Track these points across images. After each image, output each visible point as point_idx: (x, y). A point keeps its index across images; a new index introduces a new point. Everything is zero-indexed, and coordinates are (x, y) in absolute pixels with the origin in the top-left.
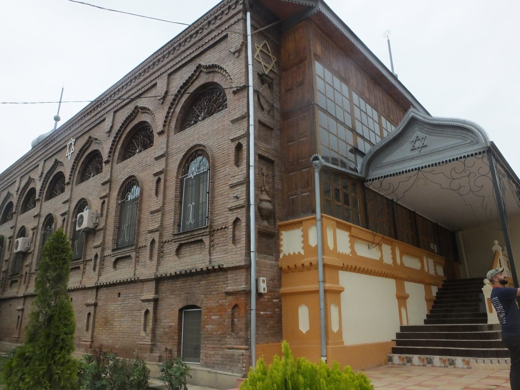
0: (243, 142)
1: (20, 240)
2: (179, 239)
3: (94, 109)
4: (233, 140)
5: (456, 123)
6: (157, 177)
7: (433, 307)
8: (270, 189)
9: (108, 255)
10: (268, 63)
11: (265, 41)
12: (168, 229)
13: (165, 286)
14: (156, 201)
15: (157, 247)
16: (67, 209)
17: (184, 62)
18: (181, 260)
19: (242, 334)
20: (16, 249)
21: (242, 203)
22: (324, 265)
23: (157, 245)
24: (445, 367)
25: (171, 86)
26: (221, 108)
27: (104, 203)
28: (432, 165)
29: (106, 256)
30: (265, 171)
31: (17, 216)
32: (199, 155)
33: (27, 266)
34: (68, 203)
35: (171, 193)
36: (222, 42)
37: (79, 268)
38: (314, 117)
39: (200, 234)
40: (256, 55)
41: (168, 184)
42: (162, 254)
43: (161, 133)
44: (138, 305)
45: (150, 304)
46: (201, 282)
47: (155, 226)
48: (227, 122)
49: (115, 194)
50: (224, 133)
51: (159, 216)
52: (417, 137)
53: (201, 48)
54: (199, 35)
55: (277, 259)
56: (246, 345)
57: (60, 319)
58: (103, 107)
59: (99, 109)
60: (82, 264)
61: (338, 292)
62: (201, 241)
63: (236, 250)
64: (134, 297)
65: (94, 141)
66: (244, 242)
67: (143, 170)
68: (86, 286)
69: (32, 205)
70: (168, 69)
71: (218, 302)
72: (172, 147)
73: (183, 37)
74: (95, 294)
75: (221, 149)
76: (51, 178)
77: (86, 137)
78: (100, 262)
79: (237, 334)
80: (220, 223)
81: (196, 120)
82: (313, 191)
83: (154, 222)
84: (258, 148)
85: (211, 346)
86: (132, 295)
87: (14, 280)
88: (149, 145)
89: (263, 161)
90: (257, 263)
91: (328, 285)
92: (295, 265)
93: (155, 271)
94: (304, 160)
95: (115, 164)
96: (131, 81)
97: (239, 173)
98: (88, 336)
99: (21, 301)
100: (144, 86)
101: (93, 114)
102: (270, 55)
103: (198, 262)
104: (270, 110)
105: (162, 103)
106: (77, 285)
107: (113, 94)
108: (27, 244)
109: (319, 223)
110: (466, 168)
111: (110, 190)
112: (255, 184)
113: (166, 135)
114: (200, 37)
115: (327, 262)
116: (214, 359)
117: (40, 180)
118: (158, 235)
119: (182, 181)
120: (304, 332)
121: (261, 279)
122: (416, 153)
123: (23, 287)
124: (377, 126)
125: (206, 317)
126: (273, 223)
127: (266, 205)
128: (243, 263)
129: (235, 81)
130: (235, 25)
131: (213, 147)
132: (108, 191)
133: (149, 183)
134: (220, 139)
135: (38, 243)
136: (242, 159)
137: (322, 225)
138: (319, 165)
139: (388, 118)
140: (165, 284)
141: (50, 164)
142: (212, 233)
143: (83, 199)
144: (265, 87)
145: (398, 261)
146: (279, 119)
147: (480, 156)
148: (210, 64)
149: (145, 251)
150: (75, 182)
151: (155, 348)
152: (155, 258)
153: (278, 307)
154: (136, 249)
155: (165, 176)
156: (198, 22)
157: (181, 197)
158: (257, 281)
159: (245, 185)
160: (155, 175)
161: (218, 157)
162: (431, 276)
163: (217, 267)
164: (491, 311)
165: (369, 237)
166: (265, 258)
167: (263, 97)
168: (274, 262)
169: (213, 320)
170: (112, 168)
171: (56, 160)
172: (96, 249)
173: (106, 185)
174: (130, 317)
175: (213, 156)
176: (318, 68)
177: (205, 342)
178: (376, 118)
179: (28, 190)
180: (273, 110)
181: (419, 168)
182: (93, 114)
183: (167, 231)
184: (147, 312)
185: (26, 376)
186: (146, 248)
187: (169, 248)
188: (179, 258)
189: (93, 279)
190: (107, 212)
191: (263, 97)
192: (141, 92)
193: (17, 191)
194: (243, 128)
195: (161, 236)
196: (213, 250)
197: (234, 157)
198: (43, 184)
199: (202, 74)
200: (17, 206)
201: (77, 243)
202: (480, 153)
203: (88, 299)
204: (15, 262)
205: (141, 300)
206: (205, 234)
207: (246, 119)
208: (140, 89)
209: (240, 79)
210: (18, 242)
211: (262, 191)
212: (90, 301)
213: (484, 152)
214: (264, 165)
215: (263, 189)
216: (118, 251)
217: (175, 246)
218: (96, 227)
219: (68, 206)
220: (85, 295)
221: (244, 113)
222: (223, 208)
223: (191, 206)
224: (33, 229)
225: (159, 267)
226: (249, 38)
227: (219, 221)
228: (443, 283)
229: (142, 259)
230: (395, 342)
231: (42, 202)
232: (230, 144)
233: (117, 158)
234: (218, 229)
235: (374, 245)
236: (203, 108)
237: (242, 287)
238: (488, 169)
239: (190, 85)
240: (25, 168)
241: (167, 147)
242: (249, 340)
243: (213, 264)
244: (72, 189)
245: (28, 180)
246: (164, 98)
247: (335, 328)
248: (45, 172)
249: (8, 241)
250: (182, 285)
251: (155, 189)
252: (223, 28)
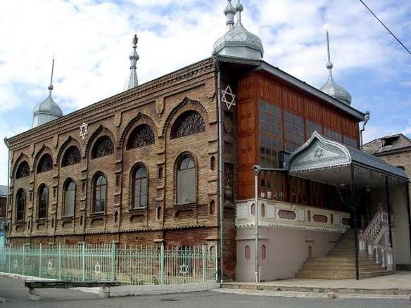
0: (216, 156)
13: (169, 235)
37: (102, 219)
111: (122, 168)
127: (229, 192)
128: (216, 225)
141: (64, 139)
193: (33, 154)
249: (28, 193)
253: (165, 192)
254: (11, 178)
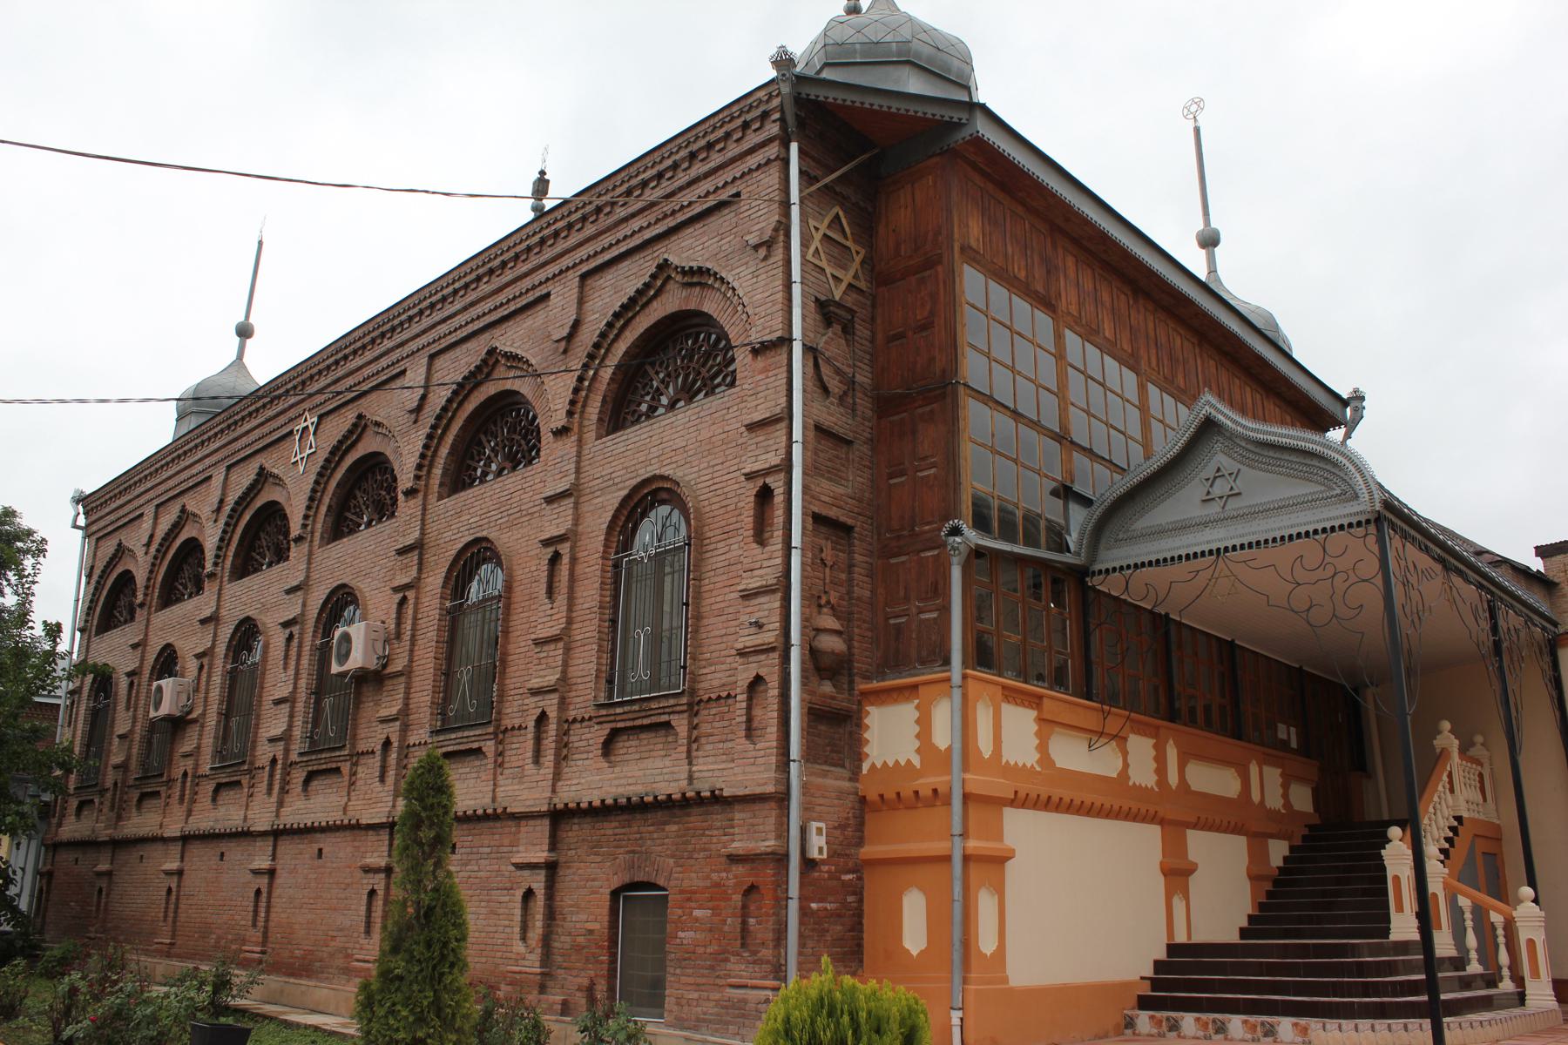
0: (776, 483)
1: (167, 684)
2: (612, 718)
3: (373, 341)
4: (750, 476)
5: (1307, 445)
6: (551, 549)
7: (1270, 894)
8: (841, 598)
9: (420, 743)
10: (844, 268)
11: (837, 209)
12: (580, 687)
13: (574, 832)
14: (549, 612)
15: (554, 733)
16: (298, 610)
17: (623, 248)
18: (617, 770)
19: (766, 953)
20: (157, 709)
21: (773, 640)
22: (966, 797)
23: (552, 727)
24: (1253, 1041)
25: (588, 306)
26: (721, 377)
27: (404, 601)
28: (1250, 545)
29: (414, 745)
30: (828, 555)
31: (149, 614)
32: (663, 502)
33: (186, 756)
34: (299, 593)
35: (590, 594)
36: (727, 211)
37: (337, 770)
38: (955, 406)
39: (663, 707)
40: (812, 249)
41: (579, 569)
42: (565, 751)
43: (561, 432)
44: (503, 875)
45: (538, 874)
46: (668, 828)
47: (547, 678)
48: (736, 425)
49: (434, 581)
50: (727, 453)
51: (556, 652)
52: (1219, 470)
53: (671, 218)
54: (664, 183)
55: (855, 775)
56: (775, 978)
57: (446, 914)
58: (398, 338)
59: (388, 344)
60: (346, 761)
61: (999, 861)
62: (667, 725)
63: (754, 754)
64: (493, 855)
65: (372, 429)
66: (775, 736)
67: (511, 526)
68: (363, 821)
69: (189, 585)
70: (582, 261)
71: (708, 877)
72: (592, 472)
73: (623, 182)
74: (387, 842)
75: (719, 492)
76: (247, 517)
77: (348, 417)
78: (399, 760)
79: (754, 953)
80: (716, 683)
81: (654, 404)
82: (946, 609)
83: (544, 666)
84: (813, 497)
85: (691, 980)
86: (488, 850)
87: (149, 790)
88: (527, 454)
89: (823, 529)
90: (805, 787)
91: (973, 844)
92: (898, 794)
93: (549, 794)
94: (927, 528)
95: (433, 498)
96: (478, 279)
97: (766, 564)
98: (371, 947)
99: (176, 849)
100: (515, 298)
101: (369, 355)
102: (848, 244)
103: (658, 778)
104: (845, 393)
105: (565, 352)
106: (336, 817)
107: (426, 308)
108: (184, 697)
109: (957, 693)
110: (1328, 559)
111: (420, 570)
112: (803, 590)
113: (574, 438)
114: (669, 190)
115: (971, 788)
116: (699, 1009)
117: (216, 521)
118: (556, 701)
119: (617, 565)
120: (915, 953)
121: (814, 825)
122: (1214, 509)
123: (178, 812)
124: (1134, 414)
125: (680, 912)
126: (846, 686)
128: (770, 789)
129: (758, 323)
130: (760, 172)
131: (699, 486)
132: (414, 573)
133: (530, 567)
134: (716, 468)
135: (215, 694)
136: (772, 525)
137: (965, 696)
138: (962, 547)
139: (1167, 386)
140: (575, 827)
141: (244, 478)
142: (696, 708)
143: (344, 586)
144: (835, 334)
145: (1173, 779)
146: (869, 413)
147: (1360, 531)
148: (694, 264)
149: (521, 739)
150: (317, 535)
151: (550, 984)
152: (549, 759)
153: (854, 893)
154: (495, 734)
155: (572, 548)
156: (664, 150)
157: (615, 607)
158: (803, 831)
159: (779, 595)
160: (547, 543)
161: (711, 514)
162: (1272, 815)
163: (708, 794)
164: (1400, 909)
165: (1091, 720)
166: (825, 774)
167: (828, 361)
168: (846, 785)
169: (697, 920)
170: (424, 509)
171: (262, 468)
172: (385, 726)
173: (410, 555)
174: (483, 904)
175: (697, 510)
176: (972, 283)
177: (678, 971)
178: (1131, 391)
179: (178, 542)
180: (854, 390)
181: (1218, 549)
182: (369, 355)
183: (578, 693)
184: (529, 894)
185: (398, 1007)
186: (523, 732)
187: (583, 737)
188: (612, 765)
189: (380, 805)
190: (414, 629)
191: (828, 361)
192: (506, 313)
193: (148, 545)
194: (774, 447)
195: (563, 704)
196: (697, 750)
197: (751, 519)
198: (225, 532)
199: (671, 286)
200: (147, 587)
201: (332, 708)
202: (1359, 524)
203: (368, 855)
204: (148, 742)
205: (513, 864)
206: (678, 708)
207: (783, 424)
208: (502, 305)
209: (769, 318)
210: (160, 689)
211: (820, 606)
212: (372, 860)
213: (1368, 522)
214: (827, 539)
215: (823, 602)
216: (448, 737)
217: (600, 733)
218: (385, 666)
219: (300, 601)
220: (357, 844)
221: (778, 410)
222: (724, 646)
223: (641, 636)
224: (199, 656)
225: (560, 783)
226: (795, 212)
227: (713, 679)
228: (1306, 832)
229: (512, 759)
230: (1148, 982)
231: (221, 582)
232: (743, 484)
233: (438, 482)
234: (710, 698)
235: (1103, 740)
236: (673, 374)
237: (767, 843)
238: (1376, 564)
239: (638, 312)
240: (171, 483)
241: (578, 471)
242: (783, 968)
243: (698, 785)
244: (310, 554)
245: (179, 517)
246: (570, 337)
247: (987, 944)
248: (231, 499)
249: (123, 683)
250: (617, 831)
251: (545, 580)
252: (728, 175)
253: (568, 650)
254: (82, 630)
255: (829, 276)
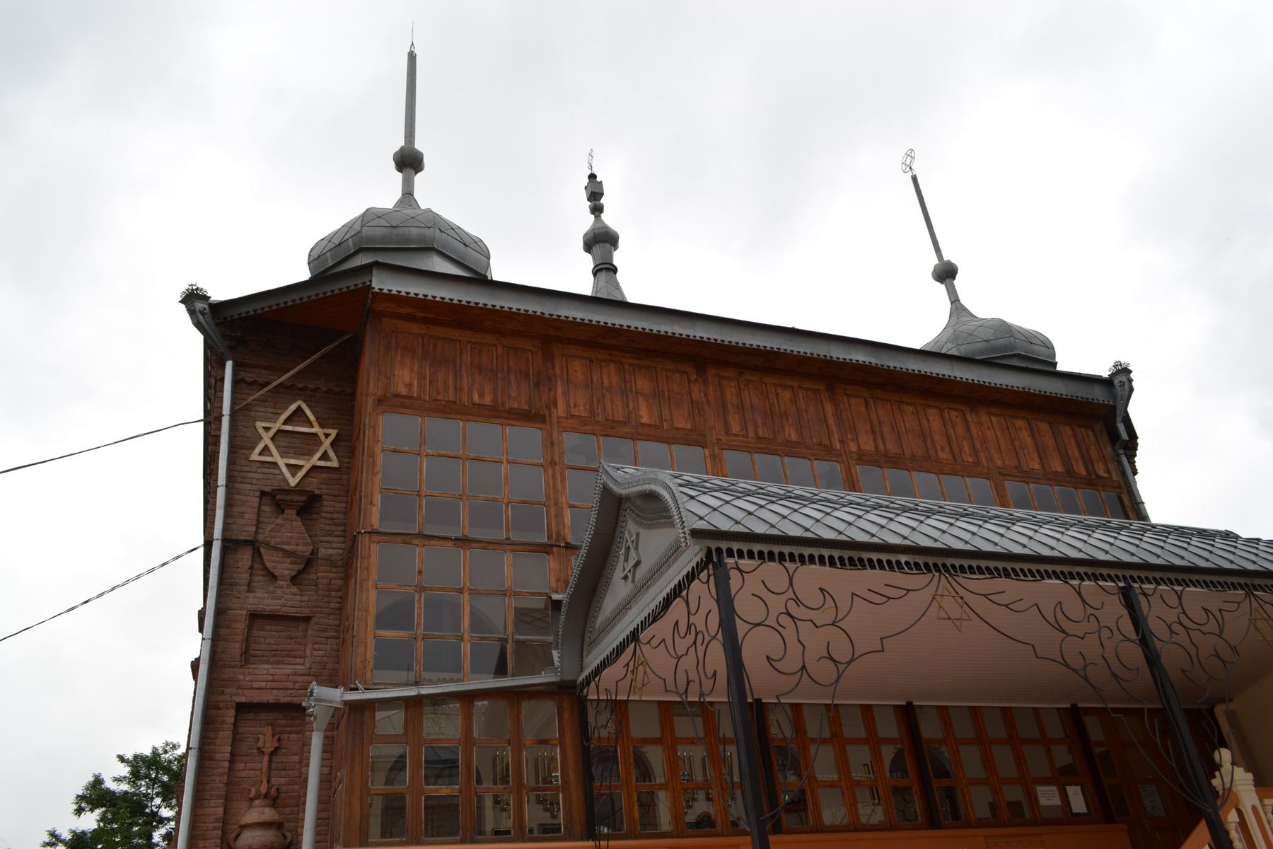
255: (284, 470)
